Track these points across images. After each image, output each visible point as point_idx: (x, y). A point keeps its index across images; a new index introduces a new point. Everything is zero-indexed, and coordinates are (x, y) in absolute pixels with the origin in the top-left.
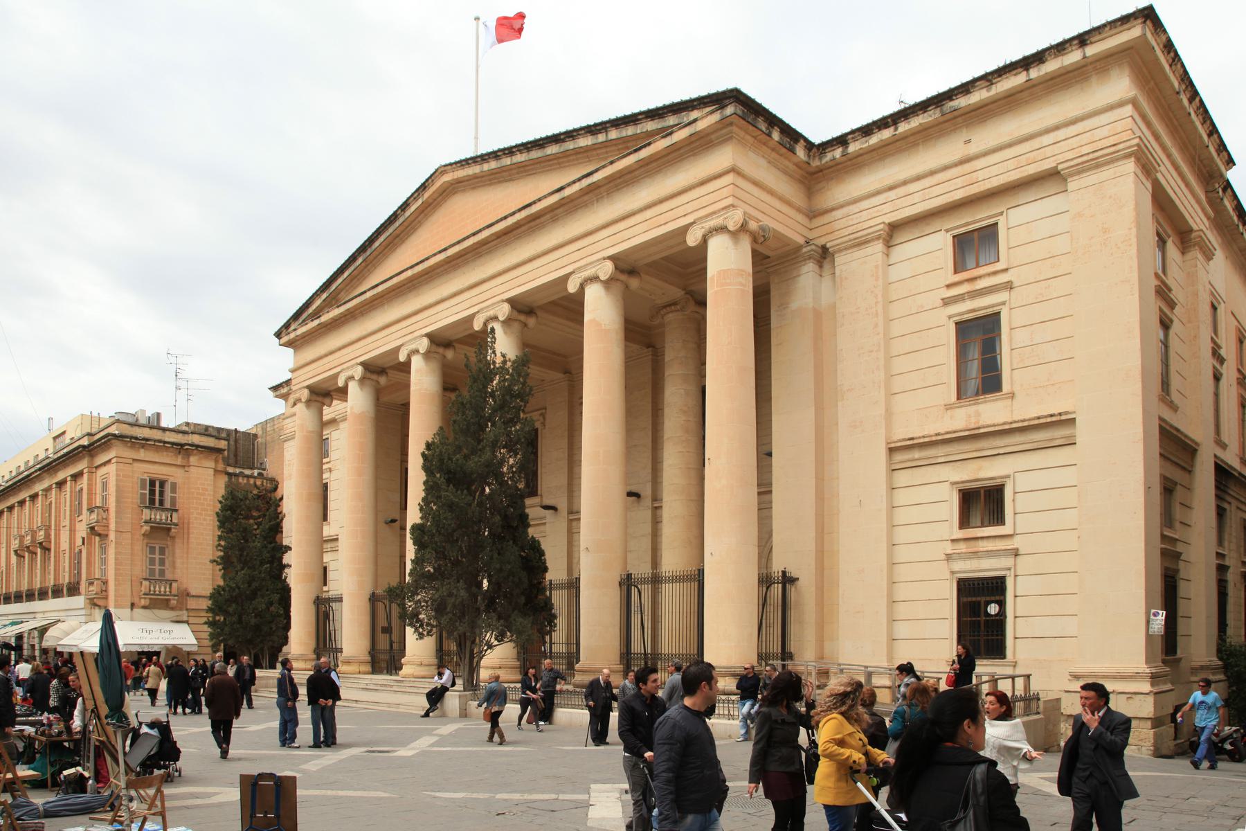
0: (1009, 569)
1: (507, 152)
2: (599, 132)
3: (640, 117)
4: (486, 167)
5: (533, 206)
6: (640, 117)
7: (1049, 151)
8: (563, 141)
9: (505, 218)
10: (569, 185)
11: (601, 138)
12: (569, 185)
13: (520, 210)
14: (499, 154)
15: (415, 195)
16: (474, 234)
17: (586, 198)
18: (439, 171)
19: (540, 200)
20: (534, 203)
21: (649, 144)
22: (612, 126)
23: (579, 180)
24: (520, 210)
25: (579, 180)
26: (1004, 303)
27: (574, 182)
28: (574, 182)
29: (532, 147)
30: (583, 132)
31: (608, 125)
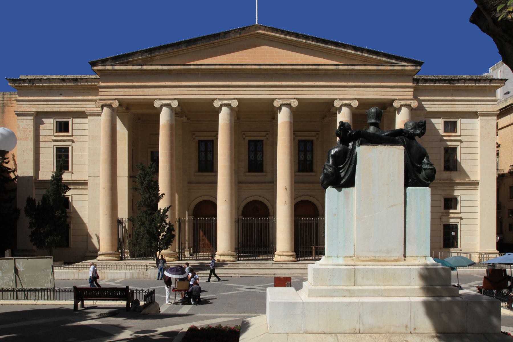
0: (459, 222)
1: (305, 36)
3: (381, 54)
6: (381, 54)
7: (476, 106)
12: (342, 65)
13: (312, 65)
14: (300, 35)
15: (236, 31)
18: (256, 26)
22: (366, 51)
24: (312, 65)
25: (348, 65)
26: (459, 145)
28: (345, 65)
30: (351, 47)
31: (365, 50)
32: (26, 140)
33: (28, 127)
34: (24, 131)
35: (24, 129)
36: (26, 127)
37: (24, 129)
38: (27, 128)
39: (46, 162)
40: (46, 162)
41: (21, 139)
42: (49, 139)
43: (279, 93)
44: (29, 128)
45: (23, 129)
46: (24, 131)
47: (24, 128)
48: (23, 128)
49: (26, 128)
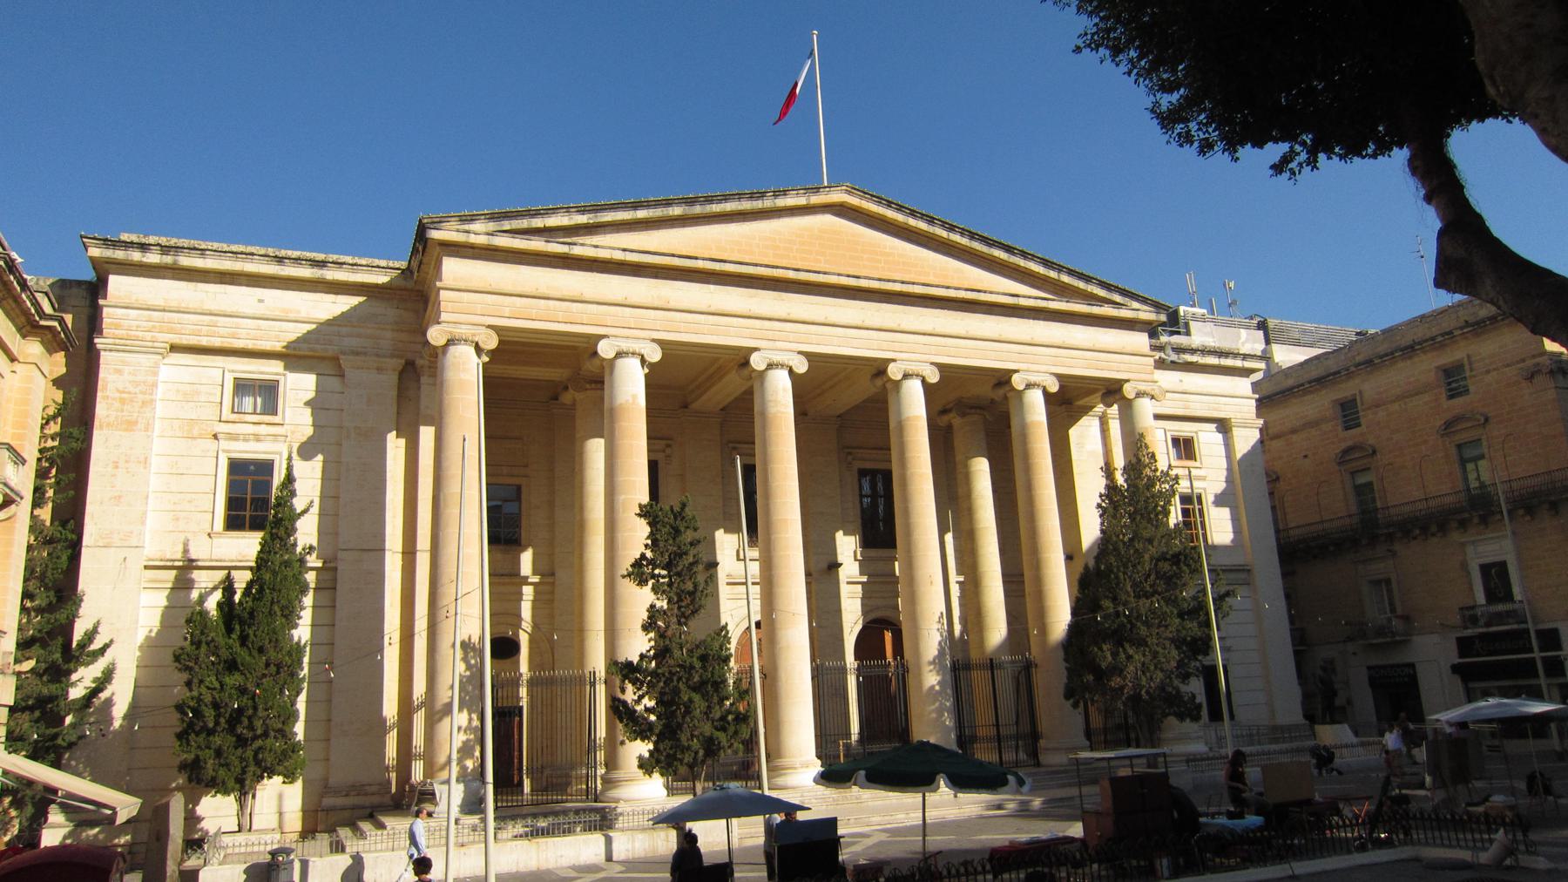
2: (1053, 269)
4: (912, 222)
5: (982, 294)
8: (1014, 254)
9: (948, 288)
10: (1024, 297)
11: (1053, 274)
12: (1024, 297)
13: (967, 290)
16: (903, 282)
17: (1027, 312)
19: (991, 293)
20: (985, 292)
21: (1101, 306)
23: (1036, 298)
24: (967, 290)
25: (1036, 298)
27: (1030, 297)
28: (1030, 297)
29: (978, 239)
32: (126, 430)
33: (137, 390)
34: (123, 401)
35: (123, 395)
36: (131, 389)
37: (126, 396)
38: (135, 393)
39: (190, 502)
40: (190, 502)
41: (108, 425)
42: (206, 430)
43: (897, 346)
44: (145, 393)
45: (118, 395)
46: (123, 401)
47: (124, 392)
48: (118, 391)
49: (129, 393)
